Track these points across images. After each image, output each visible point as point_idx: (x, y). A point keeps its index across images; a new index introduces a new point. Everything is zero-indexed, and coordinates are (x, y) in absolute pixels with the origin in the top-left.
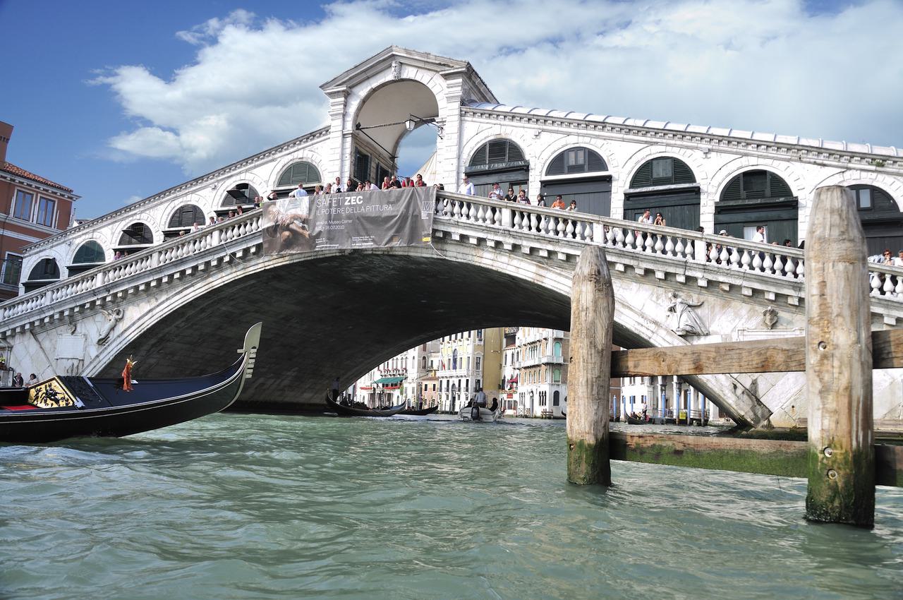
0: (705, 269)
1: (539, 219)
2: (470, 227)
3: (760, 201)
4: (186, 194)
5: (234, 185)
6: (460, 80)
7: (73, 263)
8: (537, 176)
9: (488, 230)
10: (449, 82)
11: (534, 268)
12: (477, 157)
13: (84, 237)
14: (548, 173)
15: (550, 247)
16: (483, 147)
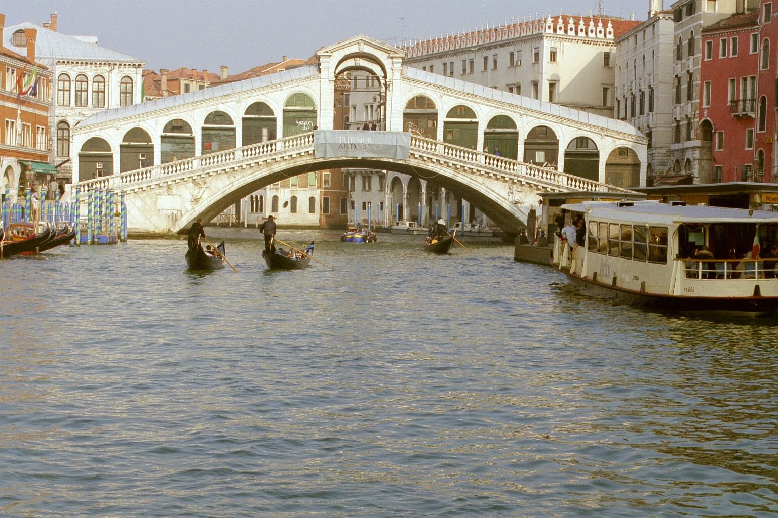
0: (525, 178)
1: (456, 151)
2: (425, 152)
3: (543, 139)
4: (217, 104)
5: (253, 102)
6: (401, 60)
7: (123, 141)
8: (442, 118)
9: (433, 155)
10: (394, 60)
11: (453, 172)
12: (410, 104)
13: (131, 125)
14: (448, 116)
15: (462, 164)
16: (413, 99)
